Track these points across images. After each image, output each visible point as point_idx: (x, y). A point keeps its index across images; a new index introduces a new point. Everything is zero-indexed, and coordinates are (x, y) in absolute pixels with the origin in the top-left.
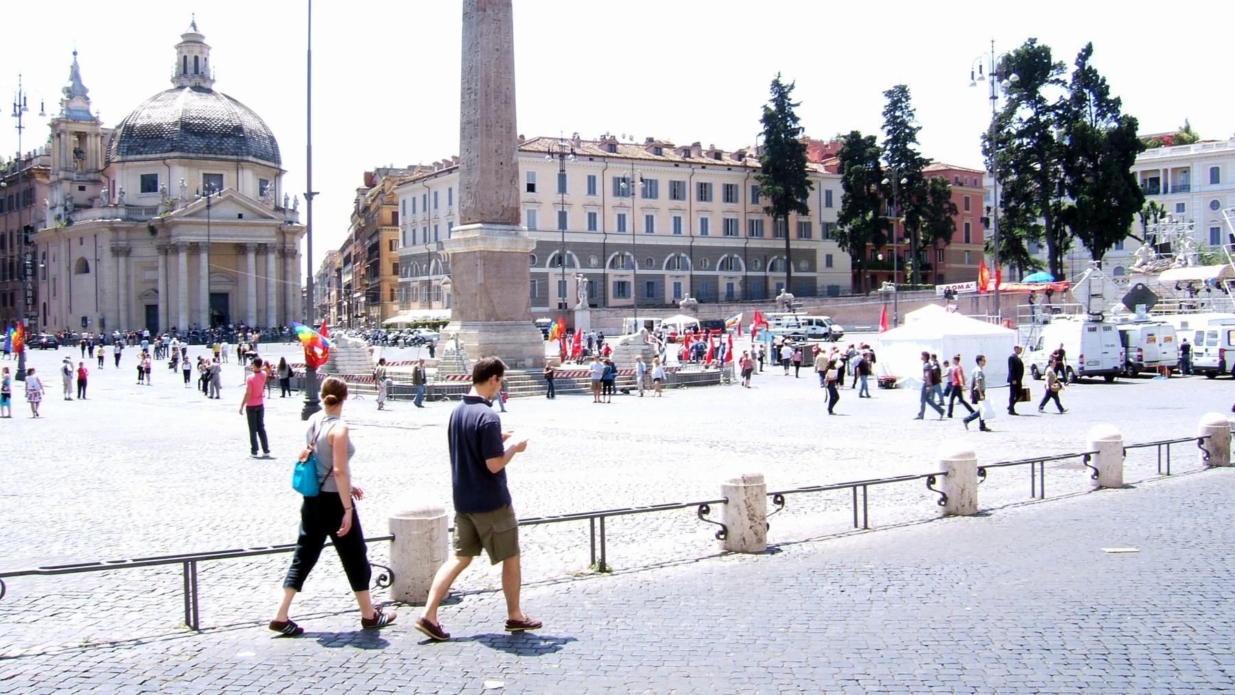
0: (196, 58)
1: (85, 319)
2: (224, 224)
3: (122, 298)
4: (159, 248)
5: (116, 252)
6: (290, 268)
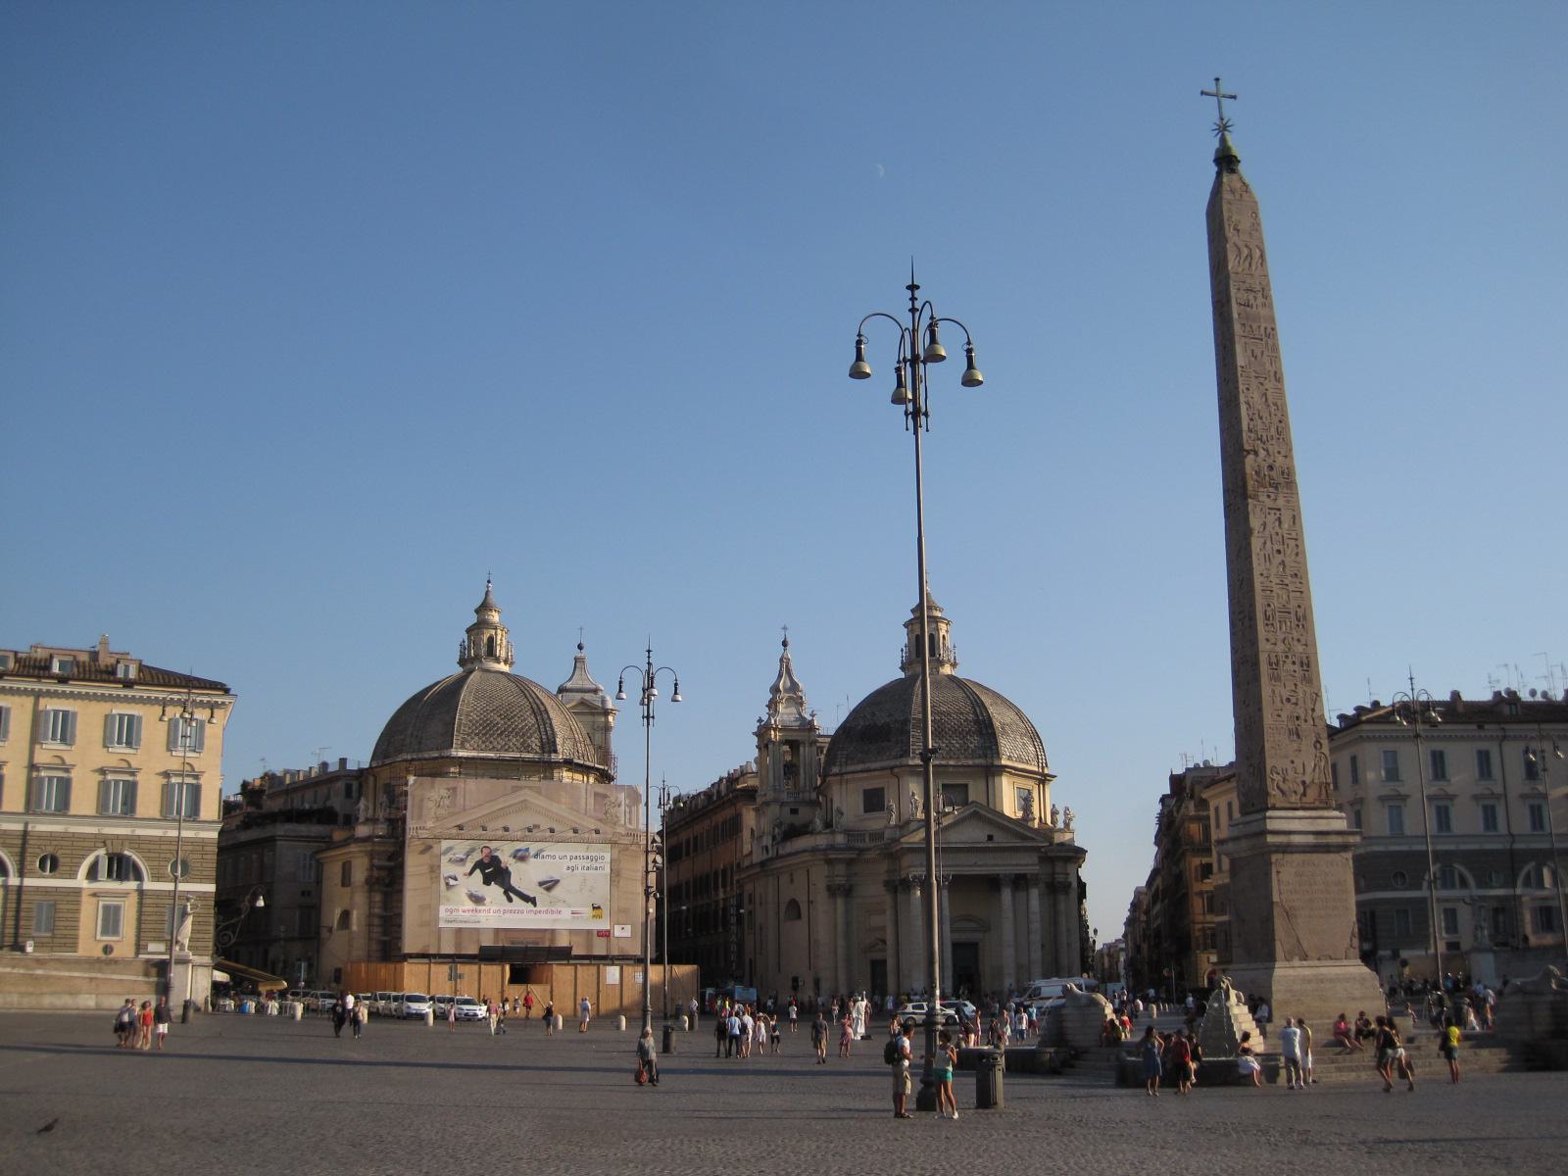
1: (795, 980)
3: (841, 951)
4: (887, 884)
5: (832, 891)
6: (1062, 907)
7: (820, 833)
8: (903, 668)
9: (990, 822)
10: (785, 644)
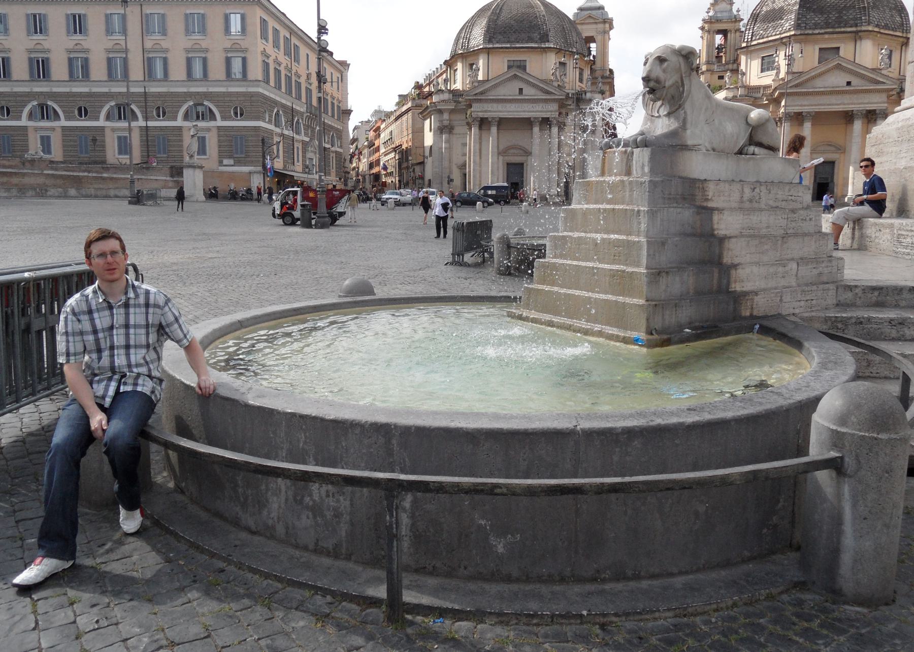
2: (831, 93)
9: (851, 72)
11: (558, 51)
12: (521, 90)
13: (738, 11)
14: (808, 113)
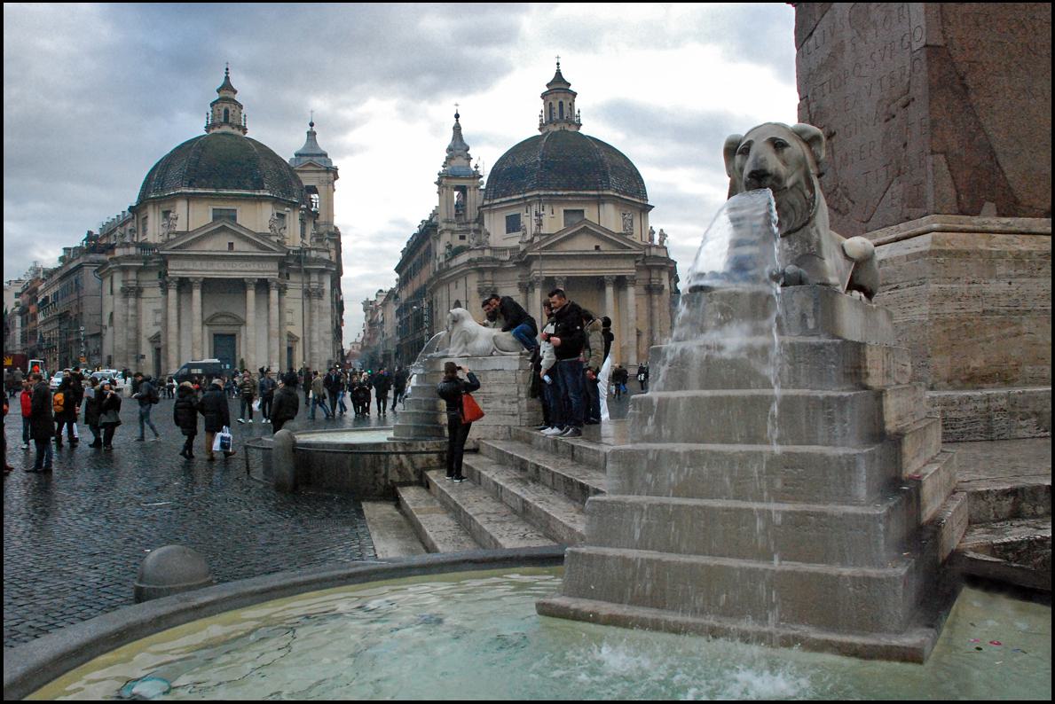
0: (561, 104)
4: (520, 285)
6: (656, 304)
7: (473, 249)
8: (540, 129)
9: (599, 236)
10: (457, 116)
11: (275, 201)
12: (231, 245)
13: (476, 167)
14: (560, 278)
